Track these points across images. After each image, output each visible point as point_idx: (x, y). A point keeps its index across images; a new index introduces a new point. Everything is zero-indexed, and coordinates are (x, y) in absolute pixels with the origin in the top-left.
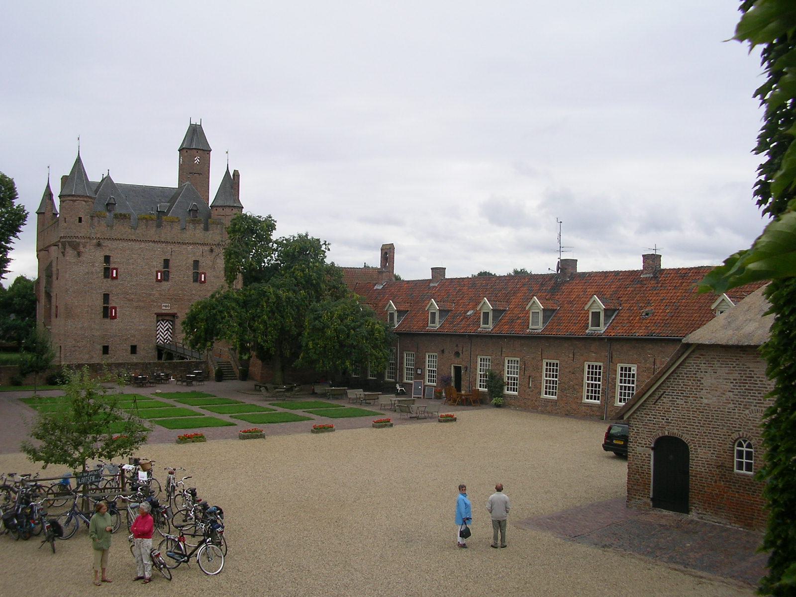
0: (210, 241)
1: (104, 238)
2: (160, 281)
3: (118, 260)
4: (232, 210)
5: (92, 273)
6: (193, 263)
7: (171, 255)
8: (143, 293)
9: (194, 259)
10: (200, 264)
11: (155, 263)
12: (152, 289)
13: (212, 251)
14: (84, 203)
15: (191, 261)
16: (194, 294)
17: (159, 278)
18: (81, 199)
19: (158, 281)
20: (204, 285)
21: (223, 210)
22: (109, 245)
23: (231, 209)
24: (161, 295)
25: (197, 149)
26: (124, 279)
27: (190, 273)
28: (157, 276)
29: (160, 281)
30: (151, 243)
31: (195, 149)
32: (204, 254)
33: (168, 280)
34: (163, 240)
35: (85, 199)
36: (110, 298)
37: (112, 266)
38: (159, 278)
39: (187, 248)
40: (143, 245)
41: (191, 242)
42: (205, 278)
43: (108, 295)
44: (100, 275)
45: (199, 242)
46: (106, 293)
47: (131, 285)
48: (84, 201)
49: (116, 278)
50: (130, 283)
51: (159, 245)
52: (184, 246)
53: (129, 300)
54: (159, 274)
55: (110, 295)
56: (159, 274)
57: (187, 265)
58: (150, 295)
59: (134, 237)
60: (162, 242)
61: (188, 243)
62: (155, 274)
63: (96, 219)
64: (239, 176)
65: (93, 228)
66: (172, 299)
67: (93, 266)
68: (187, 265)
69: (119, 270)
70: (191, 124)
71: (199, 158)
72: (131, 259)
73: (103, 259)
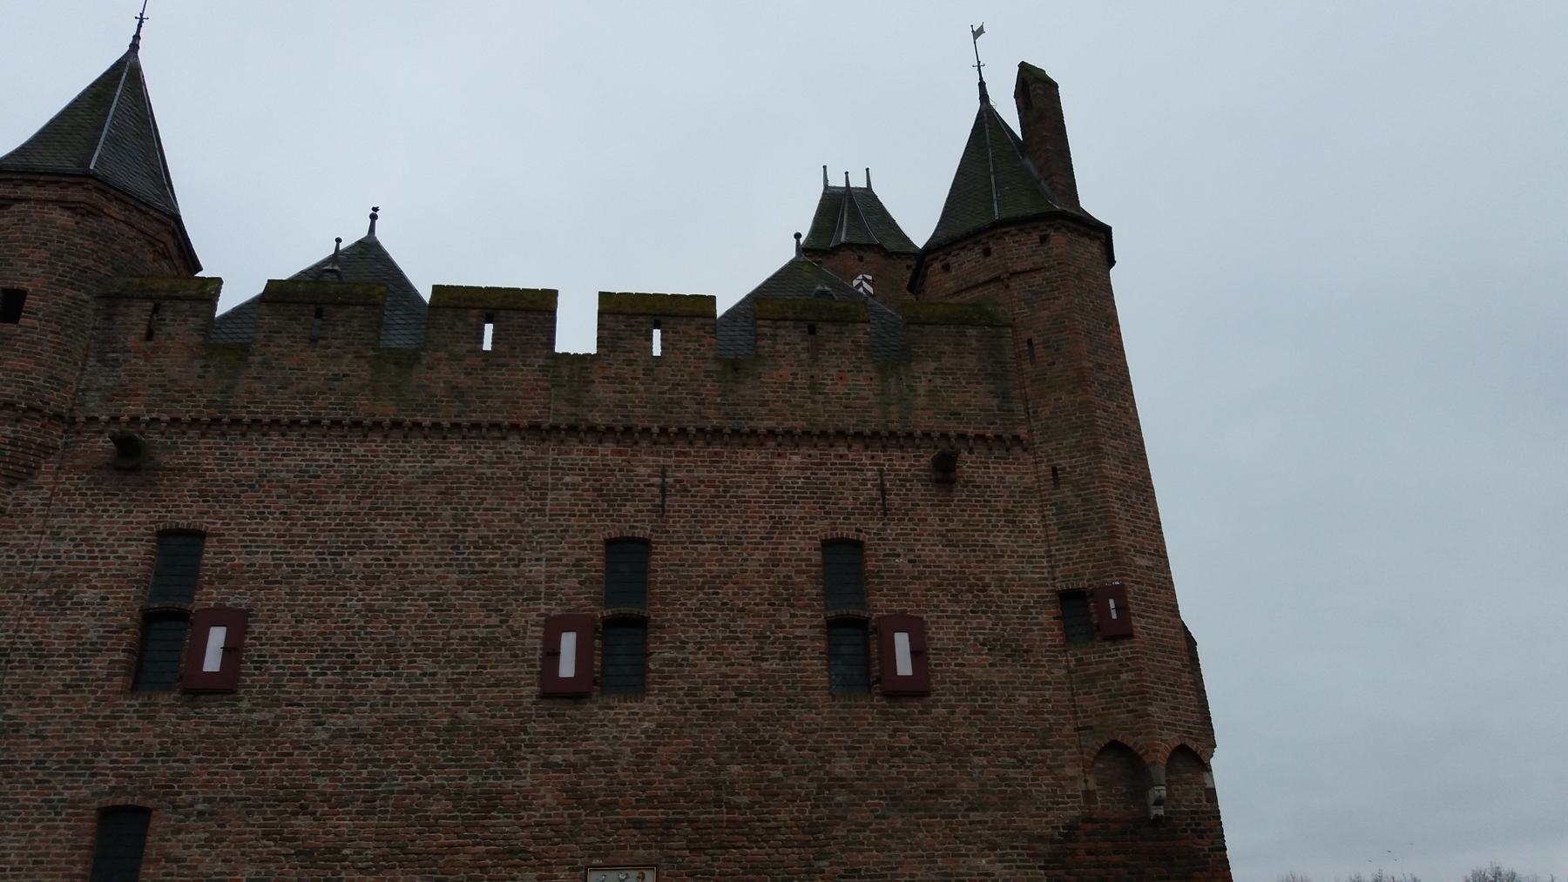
0: (923, 420)
1: (175, 421)
2: (573, 693)
3: (258, 559)
4: (1044, 239)
5: (40, 652)
6: (817, 557)
7: (661, 510)
8: (427, 793)
9: (822, 528)
10: (871, 565)
11: (538, 571)
12: (509, 758)
13: (944, 472)
14: (61, 217)
15: (802, 546)
16: (843, 783)
17: (567, 668)
18: (45, 193)
19: (555, 692)
20: (915, 706)
21: (987, 252)
22: (207, 462)
23: (1035, 236)
24: (575, 796)
25: (860, 247)
26: (292, 688)
27: (806, 625)
28: (552, 654)
29: (573, 693)
30: (513, 445)
31: (848, 246)
32: (893, 499)
33: (637, 686)
34: (599, 419)
35: (75, 194)
36: (152, 839)
37: (210, 596)
38: (567, 668)
39: (768, 467)
40: (456, 454)
41: (799, 425)
42: (917, 654)
43: (140, 816)
44: (99, 665)
45: (850, 423)
46: (121, 801)
47: (339, 734)
48: (63, 204)
49: (225, 686)
50: (336, 722)
51: (577, 453)
52: (753, 456)
53: (306, 854)
54: (568, 642)
55: (156, 824)
56: (568, 642)
57: (783, 571)
58: (490, 802)
59: (387, 410)
60: (592, 429)
61: (771, 433)
62: (534, 638)
63: (137, 316)
64: (1051, 87)
65: (103, 361)
66: (667, 827)
67: (61, 601)
68: (783, 571)
69: (257, 628)
70: (826, 186)
71: (870, 278)
72: (356, 547)
73: (137, 554)
